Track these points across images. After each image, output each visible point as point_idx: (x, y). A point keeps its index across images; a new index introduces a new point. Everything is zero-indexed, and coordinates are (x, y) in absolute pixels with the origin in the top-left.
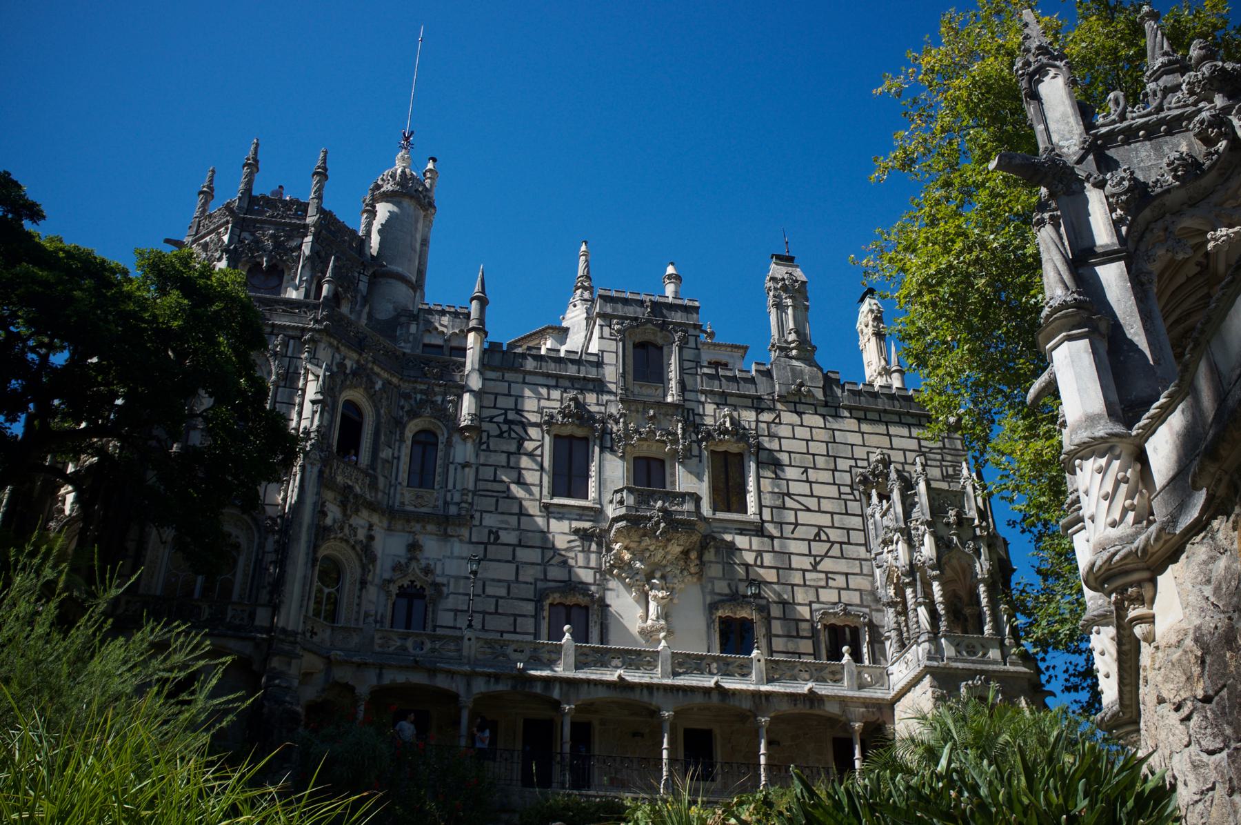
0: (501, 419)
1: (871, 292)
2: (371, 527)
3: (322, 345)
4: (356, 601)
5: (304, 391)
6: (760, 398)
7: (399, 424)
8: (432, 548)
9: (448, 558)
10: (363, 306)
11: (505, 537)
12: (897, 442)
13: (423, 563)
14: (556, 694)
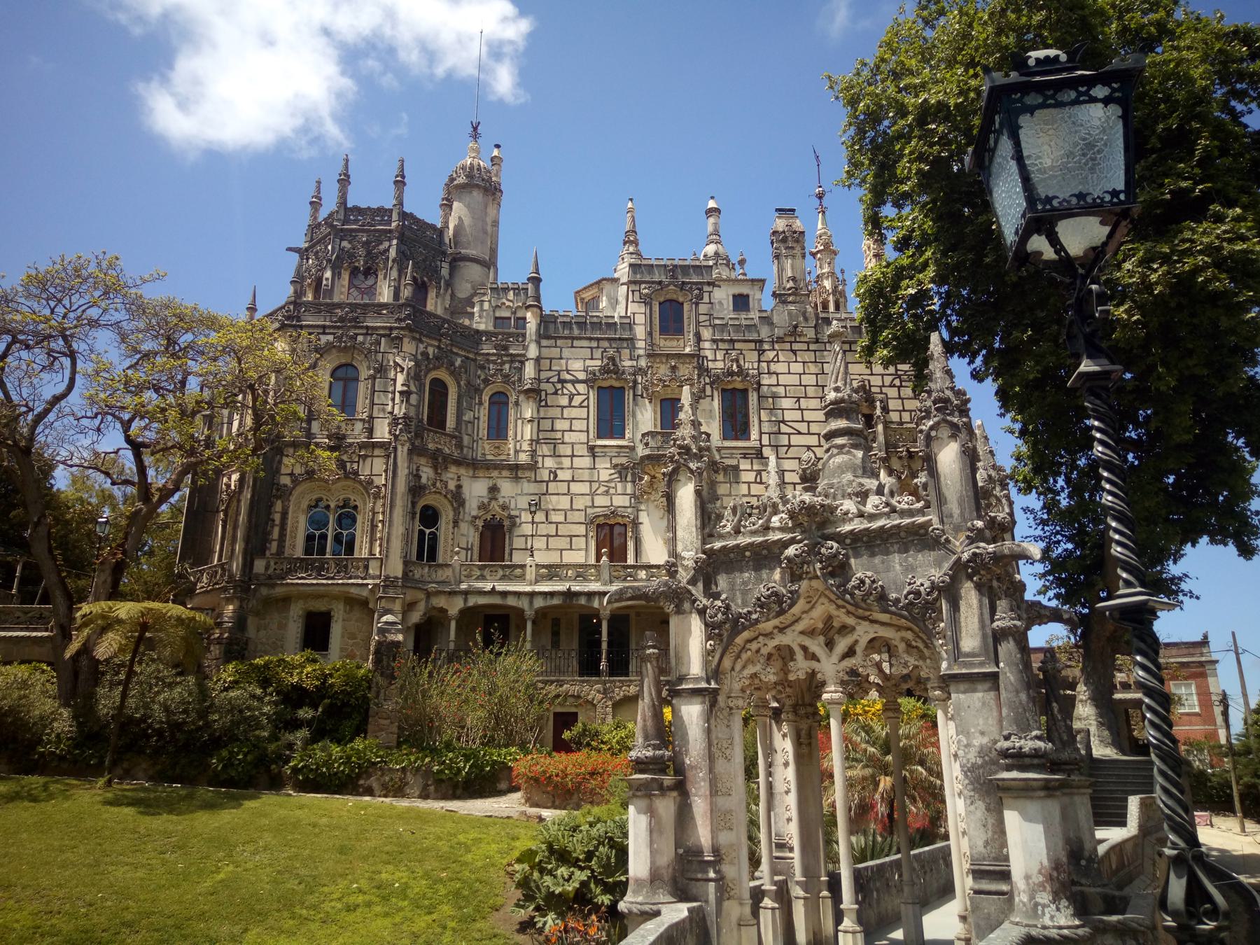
0: (555, 379)
3: (406, 340)
4: (451, 536)
5: (395, 380)
6: (761, 341)
7: (479, 391)
8: (507, 488)
10: (446, 290)
11: (562, 475)
13: (501, 501)
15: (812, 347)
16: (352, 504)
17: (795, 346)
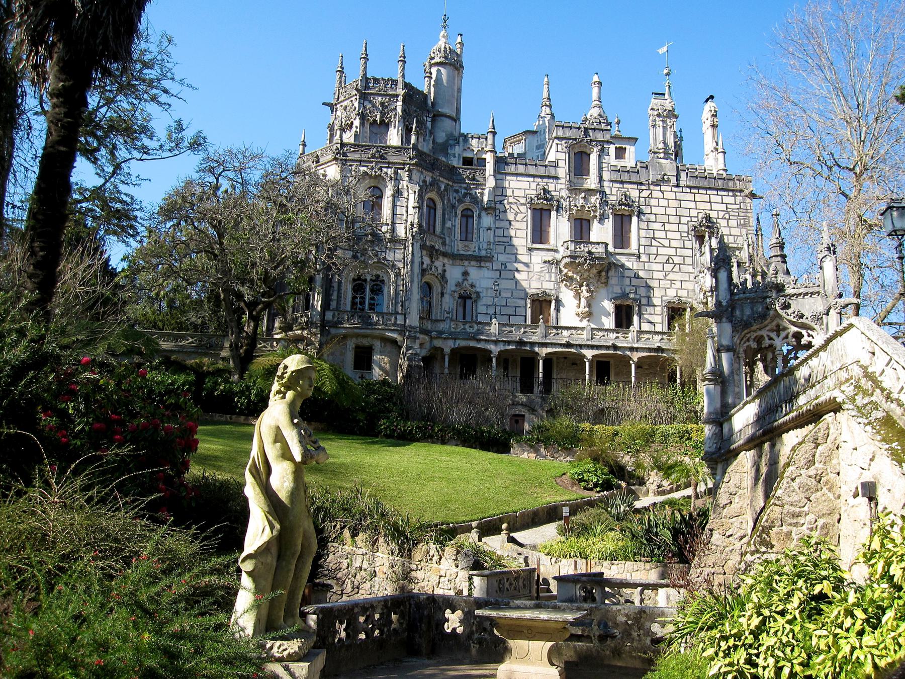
1: (712, 97)
2: (444, 265)
3: (414, 172)
6: (641, 184)
7: (453, 207)
9: (481, 278)
12: (714, 206)
13: (470, 282)
14: (536, 349)
15: (675, 189)
16: (381, 278)
17: (663, 188)
